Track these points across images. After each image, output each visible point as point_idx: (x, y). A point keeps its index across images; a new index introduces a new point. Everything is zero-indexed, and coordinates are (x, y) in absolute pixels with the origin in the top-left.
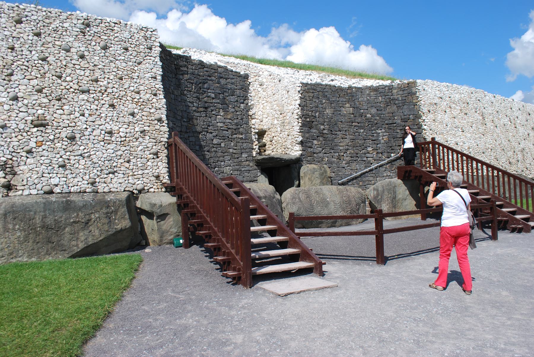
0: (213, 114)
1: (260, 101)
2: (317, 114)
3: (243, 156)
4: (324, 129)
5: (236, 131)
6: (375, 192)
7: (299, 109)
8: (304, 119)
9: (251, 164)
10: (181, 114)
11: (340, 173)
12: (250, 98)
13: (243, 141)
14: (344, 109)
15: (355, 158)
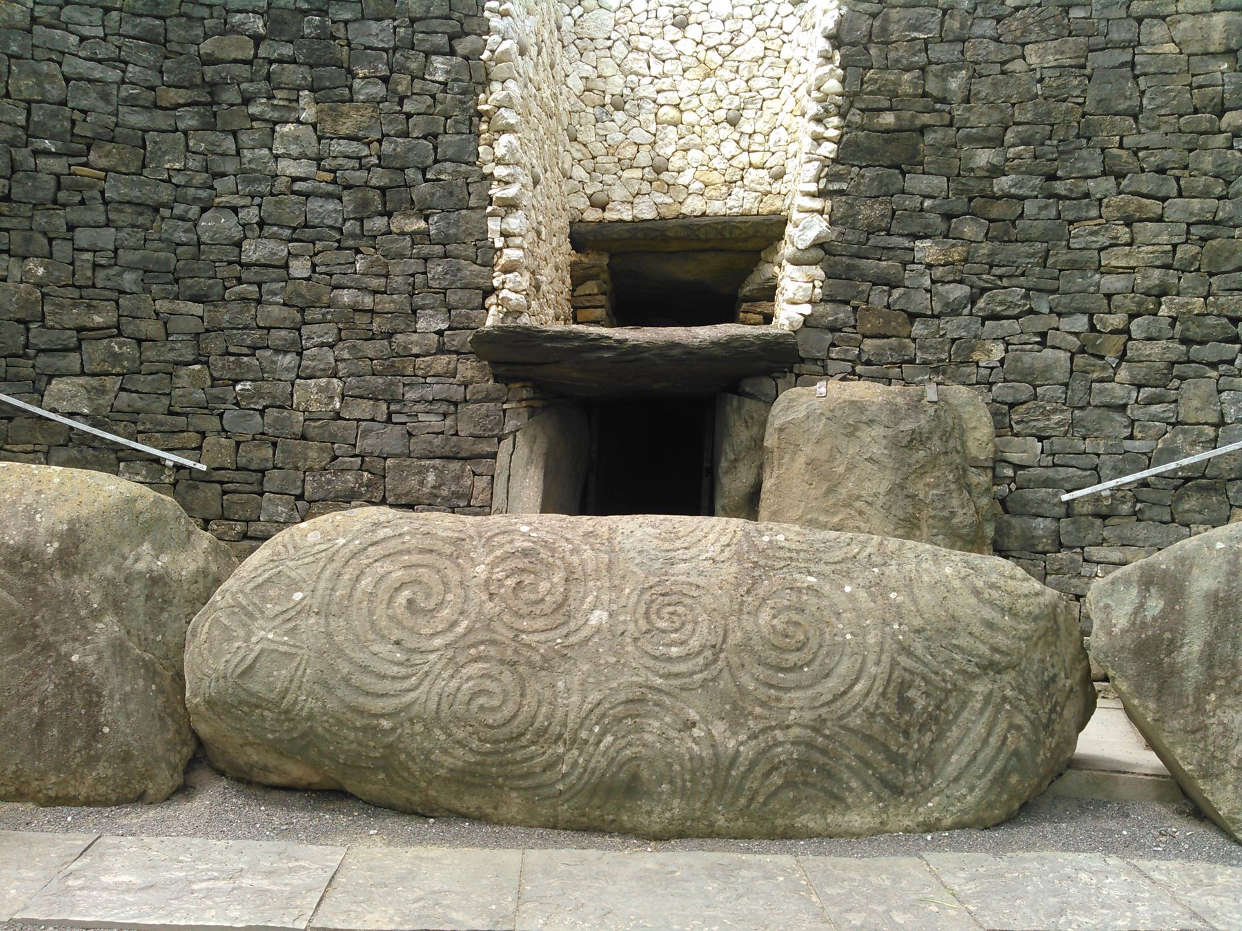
0: (253, 118)
1: (786, 79)
2: (954, 84)
3: (421, 325)
4: (995, 171)
5: (392, 199)
6: (1155, 605)
7: (829, 59)
8: (855, 117)
9: (468, 368)
10: (21, 119)
11: (1088, 445)
12: (495, 22)
13: (427, 249)
14: (1159, 30)
15: (1208, 352)
